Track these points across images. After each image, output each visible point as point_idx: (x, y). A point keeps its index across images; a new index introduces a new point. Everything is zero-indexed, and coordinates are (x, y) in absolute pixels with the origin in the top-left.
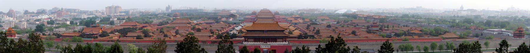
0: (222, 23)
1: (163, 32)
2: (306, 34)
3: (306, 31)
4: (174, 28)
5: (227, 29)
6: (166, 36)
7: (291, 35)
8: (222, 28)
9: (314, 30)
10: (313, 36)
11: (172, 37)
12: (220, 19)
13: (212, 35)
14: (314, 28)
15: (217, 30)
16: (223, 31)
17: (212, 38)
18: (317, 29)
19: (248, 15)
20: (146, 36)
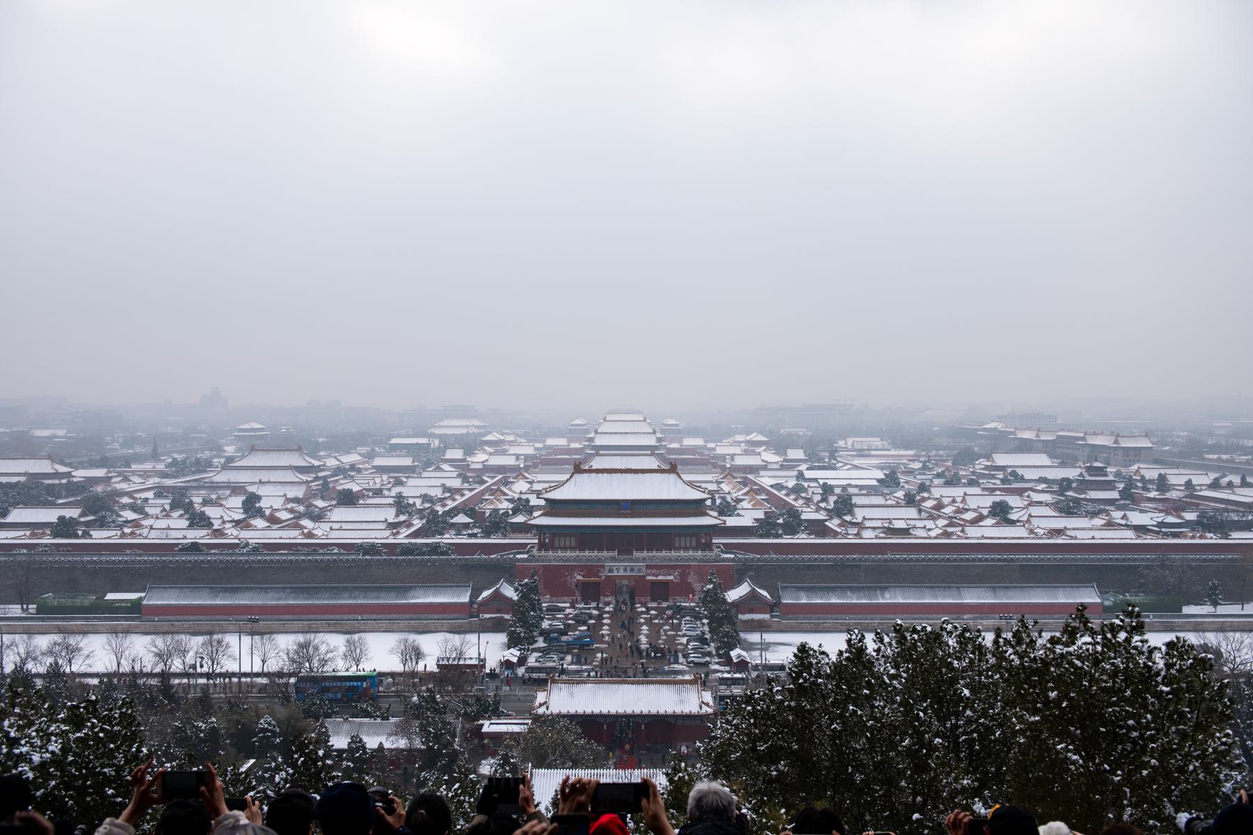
0: (445, 467)
1: (188, 508)
2: (793, 513)
3: (790, 499)
4: (236, 489)
5: (468, 494)
6: (199, 520)
7: (731, 522)
8: (446, 489)
9: (824, 500)
10: (818, 528)
11: (231, 531)
12: (442, 450)
13: (402, 518)
16: (451, 504)
17: (405, 532)
18: (838, 491)
20: (102, 524)
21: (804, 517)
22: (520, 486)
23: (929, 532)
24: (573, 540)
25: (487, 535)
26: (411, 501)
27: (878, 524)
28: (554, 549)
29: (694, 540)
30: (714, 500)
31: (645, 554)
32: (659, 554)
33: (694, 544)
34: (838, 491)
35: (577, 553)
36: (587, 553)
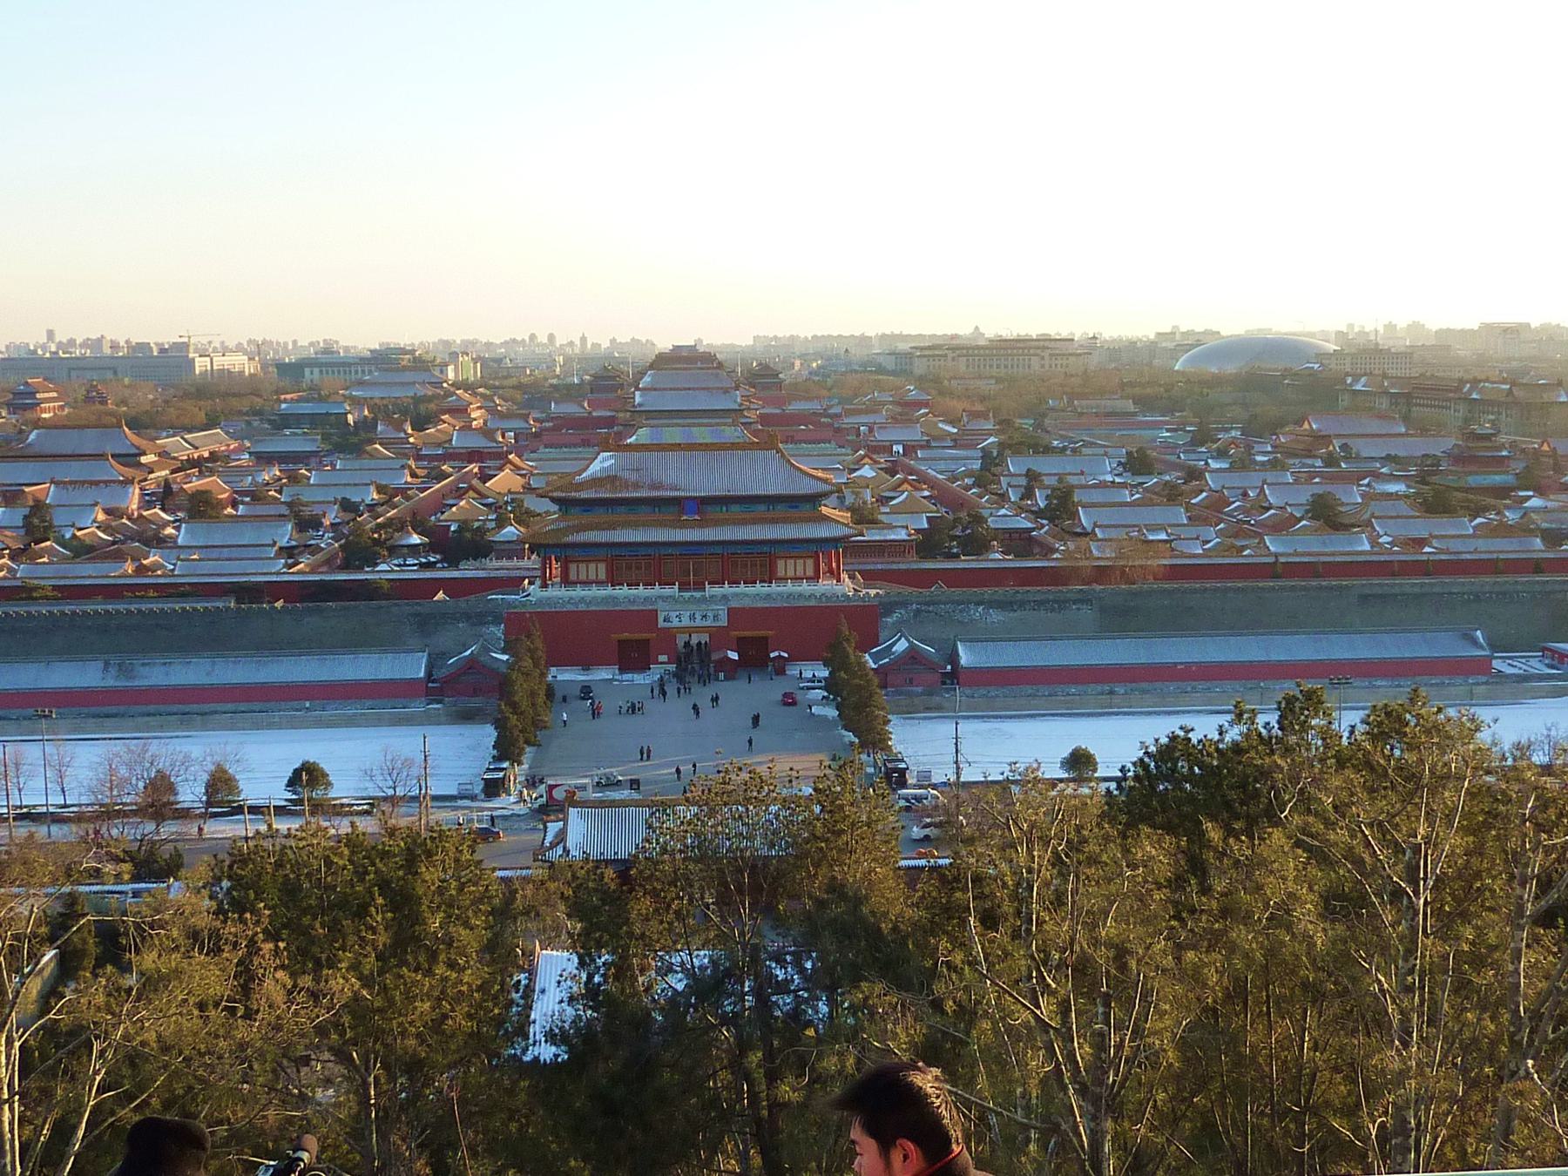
9: (1028, 493)
14: (1033, 476)
15: (347, 506)
18: (1047, 481)
19: (567, 392)
21: (992, 523)
22: (504, 481)
23: (1202, 545)
24: (602, 567)
25: (452, 561)
26: (317, 510)
27: (1121, 534)
28: (566, 581)
29: (810, 562)
30: (842, 499)
31: (727, 589)
32: (750, 590)
33: (810, 572)
34: (1047, 481)
35: (608, 591)
36: (624, 591)
